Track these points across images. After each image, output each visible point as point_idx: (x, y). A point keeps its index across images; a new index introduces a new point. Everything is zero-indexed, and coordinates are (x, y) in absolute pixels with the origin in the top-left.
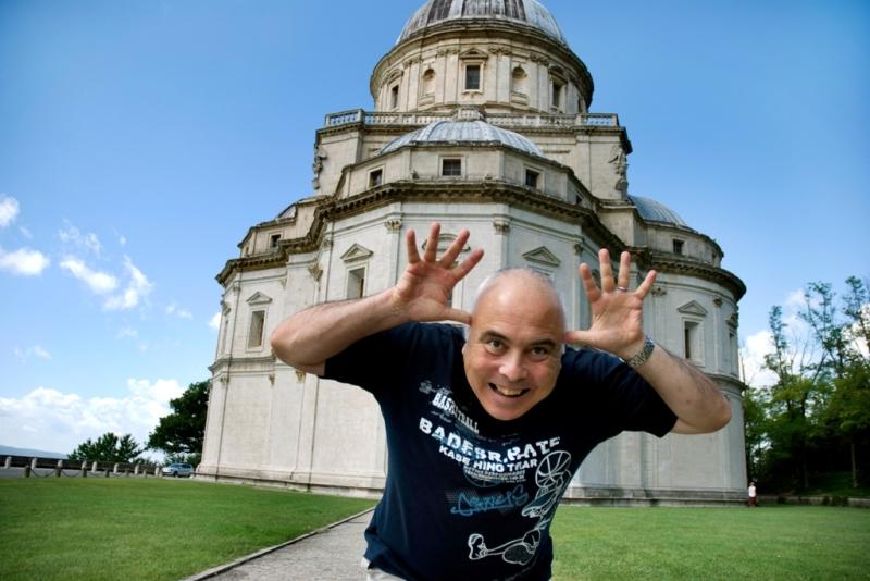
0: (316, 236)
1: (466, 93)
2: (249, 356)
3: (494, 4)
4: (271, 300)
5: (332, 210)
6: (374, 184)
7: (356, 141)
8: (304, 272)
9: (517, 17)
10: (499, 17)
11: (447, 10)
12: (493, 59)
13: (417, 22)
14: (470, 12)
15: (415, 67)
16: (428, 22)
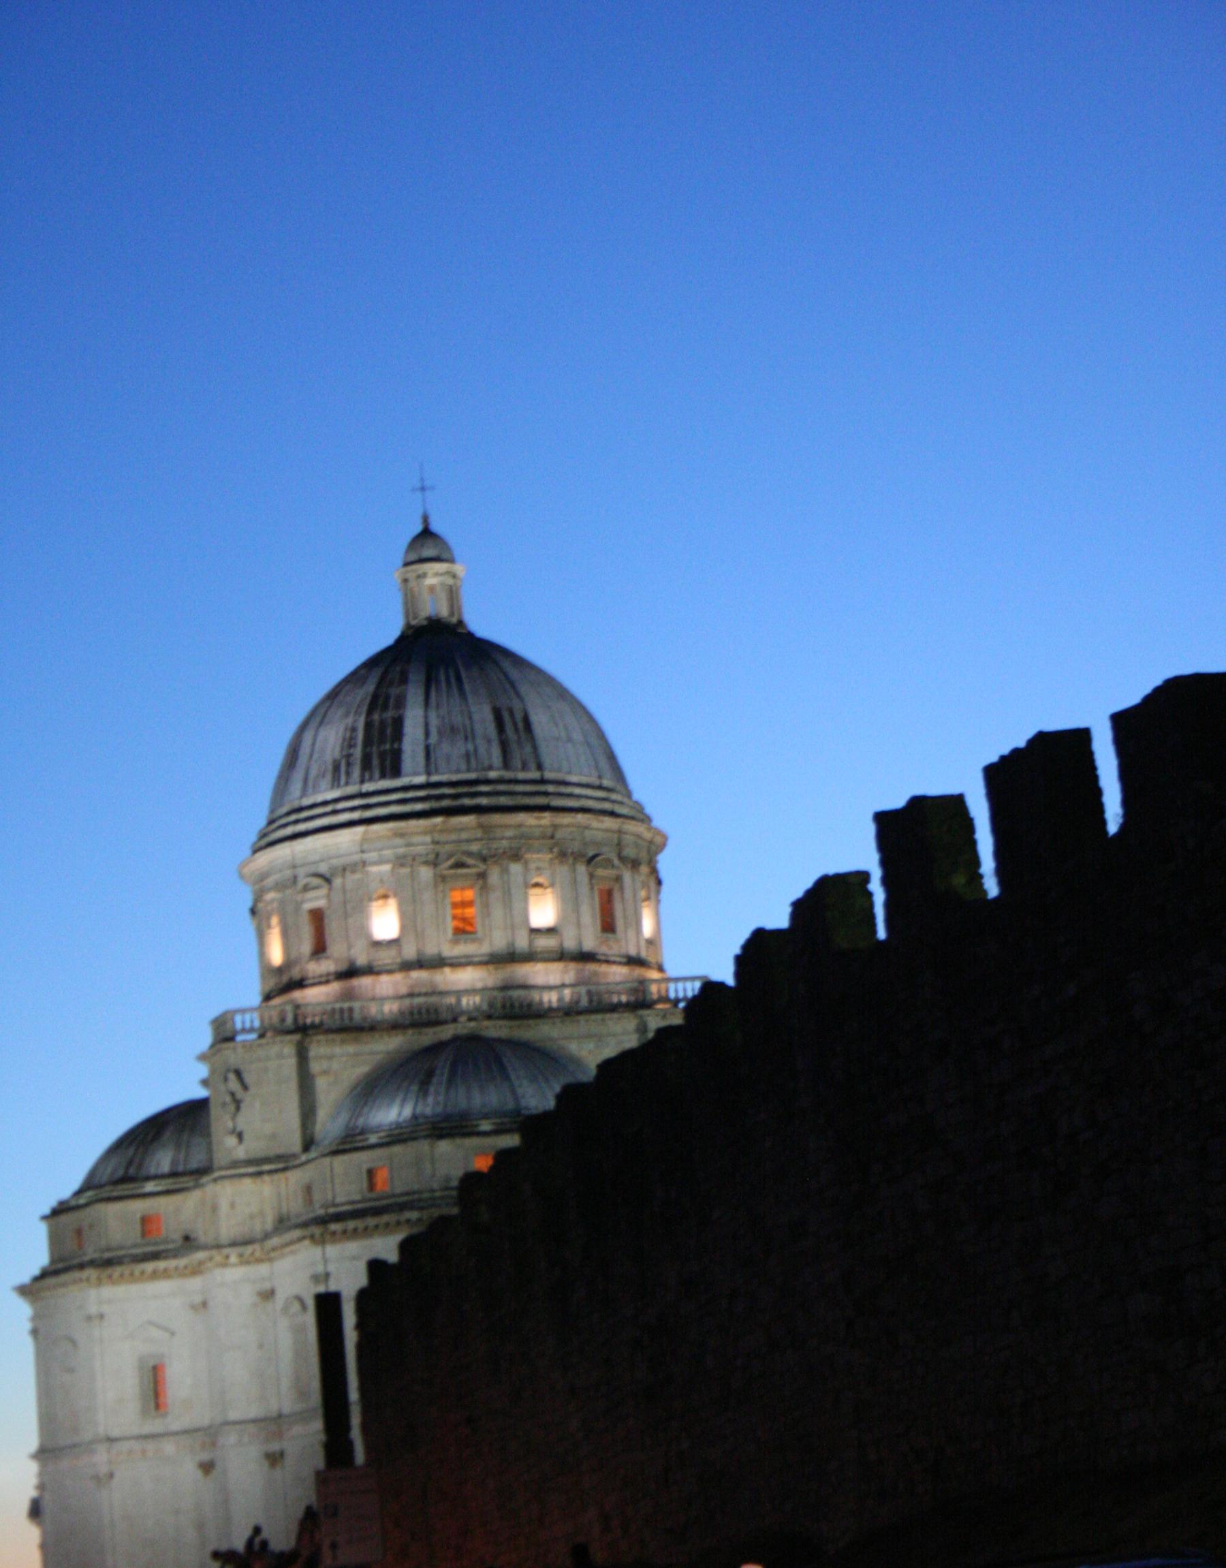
0: (274, 1249)
1: (455, 942)
2: (148, 1429)
3: (482, 750)
4: (173, 1334)
5: (322, 1235)
6: (372, 1186)
7: (292, 1062)
8: (248, 1295)
9: (525, 767)
10: (493, 775)
11: (397, 756)
12: (494, 876)
13: (336, 768)
14: (442, 764)
15: (352, 879)
16: (362, 782)
